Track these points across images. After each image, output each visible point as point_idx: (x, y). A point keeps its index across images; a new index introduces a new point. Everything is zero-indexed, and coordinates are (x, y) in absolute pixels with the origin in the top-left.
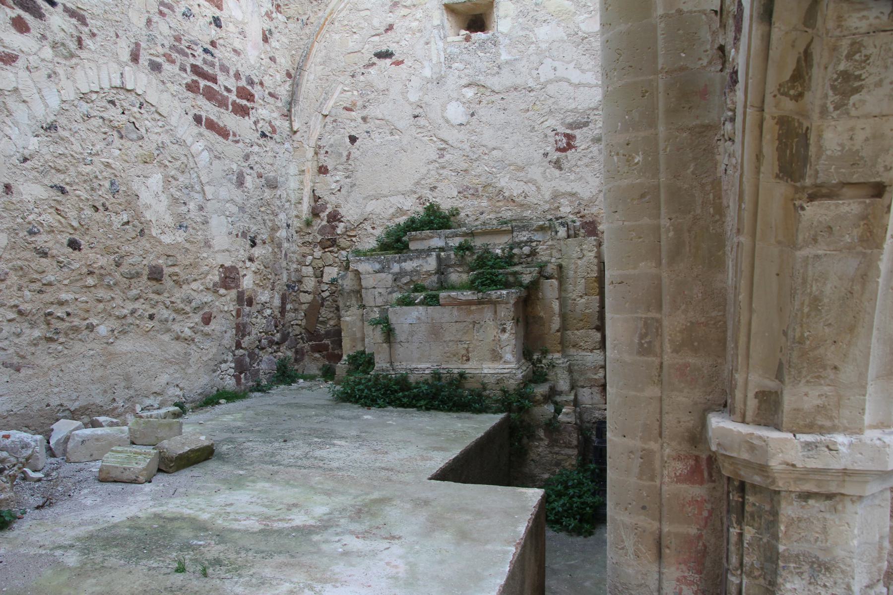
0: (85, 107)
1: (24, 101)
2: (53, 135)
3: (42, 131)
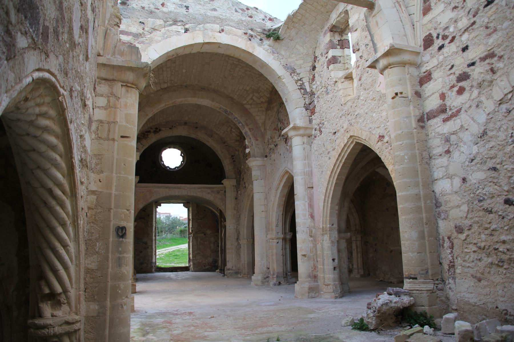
0: (504, 107)
1: (467, 129)
2: (485, 138)
3: (479, 139)
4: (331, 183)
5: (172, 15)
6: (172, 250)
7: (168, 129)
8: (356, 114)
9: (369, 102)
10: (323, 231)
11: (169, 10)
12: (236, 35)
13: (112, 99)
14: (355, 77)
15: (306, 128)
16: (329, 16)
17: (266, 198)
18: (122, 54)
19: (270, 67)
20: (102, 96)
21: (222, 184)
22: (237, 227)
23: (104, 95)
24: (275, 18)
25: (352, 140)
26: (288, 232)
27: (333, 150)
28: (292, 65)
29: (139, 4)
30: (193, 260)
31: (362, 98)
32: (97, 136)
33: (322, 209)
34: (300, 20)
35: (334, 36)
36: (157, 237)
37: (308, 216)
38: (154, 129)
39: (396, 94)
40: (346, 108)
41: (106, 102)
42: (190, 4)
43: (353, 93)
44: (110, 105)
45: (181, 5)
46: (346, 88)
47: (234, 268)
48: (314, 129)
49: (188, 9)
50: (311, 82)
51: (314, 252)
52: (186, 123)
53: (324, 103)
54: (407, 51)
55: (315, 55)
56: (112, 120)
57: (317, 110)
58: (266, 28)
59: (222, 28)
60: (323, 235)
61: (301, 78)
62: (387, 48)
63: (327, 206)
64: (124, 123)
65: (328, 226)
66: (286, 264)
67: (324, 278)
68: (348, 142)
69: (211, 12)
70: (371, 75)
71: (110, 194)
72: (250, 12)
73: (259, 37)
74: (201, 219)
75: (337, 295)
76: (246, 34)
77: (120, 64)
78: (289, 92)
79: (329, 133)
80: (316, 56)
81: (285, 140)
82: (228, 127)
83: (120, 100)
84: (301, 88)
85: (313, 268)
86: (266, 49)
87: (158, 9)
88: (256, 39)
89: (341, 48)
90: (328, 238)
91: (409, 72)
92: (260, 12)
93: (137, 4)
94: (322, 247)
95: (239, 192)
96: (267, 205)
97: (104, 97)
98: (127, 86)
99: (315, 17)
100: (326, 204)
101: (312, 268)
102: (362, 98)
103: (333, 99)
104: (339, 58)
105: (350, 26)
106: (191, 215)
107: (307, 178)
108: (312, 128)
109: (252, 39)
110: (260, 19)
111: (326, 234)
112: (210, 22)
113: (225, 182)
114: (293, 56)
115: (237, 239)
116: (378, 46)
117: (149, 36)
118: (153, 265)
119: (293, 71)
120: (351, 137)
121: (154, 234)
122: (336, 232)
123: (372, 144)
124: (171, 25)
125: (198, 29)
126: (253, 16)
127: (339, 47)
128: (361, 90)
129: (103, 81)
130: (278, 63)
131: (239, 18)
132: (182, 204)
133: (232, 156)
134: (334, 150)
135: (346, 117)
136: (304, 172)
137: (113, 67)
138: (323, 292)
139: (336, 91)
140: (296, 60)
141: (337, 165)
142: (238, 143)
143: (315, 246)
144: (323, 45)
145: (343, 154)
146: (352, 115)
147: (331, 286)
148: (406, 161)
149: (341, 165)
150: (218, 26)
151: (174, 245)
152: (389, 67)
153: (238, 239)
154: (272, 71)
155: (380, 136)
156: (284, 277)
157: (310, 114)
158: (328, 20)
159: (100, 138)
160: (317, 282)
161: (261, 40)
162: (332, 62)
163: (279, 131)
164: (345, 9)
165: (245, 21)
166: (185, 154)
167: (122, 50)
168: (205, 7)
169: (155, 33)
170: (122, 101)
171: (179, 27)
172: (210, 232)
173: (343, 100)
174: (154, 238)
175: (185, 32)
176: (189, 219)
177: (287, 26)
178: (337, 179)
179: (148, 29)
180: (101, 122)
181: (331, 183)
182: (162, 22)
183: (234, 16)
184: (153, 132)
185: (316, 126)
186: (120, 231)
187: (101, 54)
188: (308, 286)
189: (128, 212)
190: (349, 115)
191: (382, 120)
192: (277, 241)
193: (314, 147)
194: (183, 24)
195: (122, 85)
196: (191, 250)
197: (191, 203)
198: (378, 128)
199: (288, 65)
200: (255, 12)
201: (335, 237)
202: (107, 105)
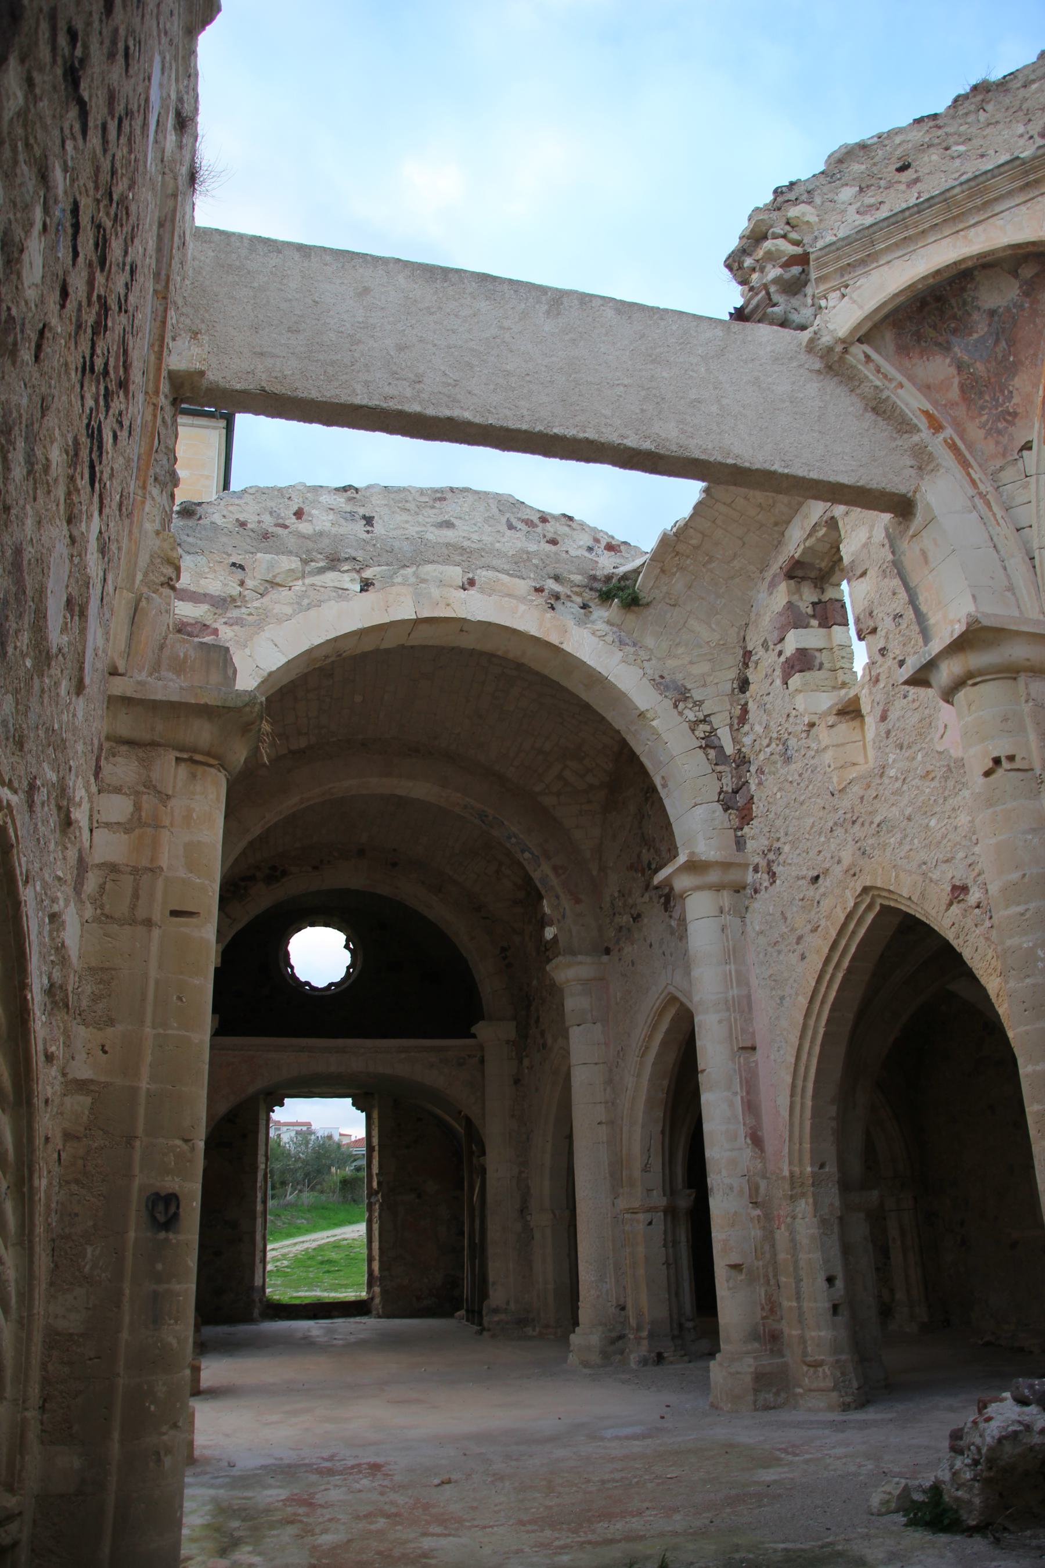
4: (810, 1033)
5: (326, 541)
6: (314, 1245)
8: (877, 820)
9: (914, 783)
10: (792, 1188)
11: (317, 528)
12: (509, 595)
13: (148, 801)
14: (869, 709)
15: (726, 866)
16: (783, 534)
17: (610, 1082)
18: (179, 667)
19: (613, 687)
20: (118, 790)
21: (474, 1036)
22: (521, 1172)
23: (125, 790)
24: (625, 543)
25: (868, 900)
26: (680, 1187)
27: (812, 931)
28: (679, 676)
29: (231, 512)
30: (382, 1279)
31: (892, 773)
32: (99, 911)
33: (787, 1117)
34: (696, 548)
35: (798, 591)
36: (270, 1203)
37: (742, 1140)
39: (997, 761)
40: (845, 803)
41: (131, 809)
42: (377, 509)
43: (866, 757)
44: (140, 819)
45: (352, 514)
46: (843, 744)
47: (512, 1306)
48: (751, 869)
49: (372, 526)
50: (736, 727)
51: (768, 1256)
52: (361, 853)
53: (780, 789)
54: (1018, 634)
55: (745, 647)
56: (145, 863)
57: (757, 809)
58: (599, 573)
59: (470, 576)
60: (793, 1198)
61: (706, 716)
62: (959, 629)
63: (803, 1105)
64: (182, 873)
65: (809, 1169)
66: (677, 1294)
67: (802, 1340)
68: (856, 905)
69: (436, 531)
70: (916, 704)
71: (134, 1091)
72: (552, 530)
73: (579, 600)
75: (848, 1399)
76: (539, 590)
77: (175, 698)
78: (673, 758)
79: (798, 878)
80: (749, 648)
81: (662, 900)
83: (173, 803)
84: (707, 746)
85: (767, 1308)
86: (599, 633)
87: (286, 527)
88: (569, 604)
89: (820, 625)
90: (810, 1209)
91: (1028, 694)
92: (578, 527)
93: (225, 513)
94: (793, 1240)
95: (526, 1062)
96: (613, 1103)
97: (125, 794)
98: (191, 760)
99: (741, 539)
100: (798, 1099)
101: (763, 1309)
102: (892, 773)
103: (806, 775)
104: (817, 654)
105: (846, 560)
106: (375, 1133)
107: (736, 1020)
108: (747, 865)
109: (558, 606)
110: (580, 547)
111: (803, 1195)
112: (436, 558)
113: (483, 1030)
114: (680, 651)
115: (522, 1211)
116: (932, 621)
117: (256, 604)
119: (682, 696)
120: (866, 890)
121: (259, 1195)
122: (835, 1190)
123: (933, 913)
124: (321, 571)
125: (399, 580)
126: (559, 539)
127: (814, 622)
128: (888, 750)
129: (124, 748)
130: (635, 672)
131: (519, 545)
132: (349, 1100)
133: (503, 950)
134: (815, 930)
135: (846, 831)
136: (726, 1001)
137: (154, 707)
138: (800, 1390)
139: (812, 753)
140: (691, 663)
141: (828, 977)
143: (769, 1237)
144: (768, 619)
145: (843, 942)
146: (867, 824)
147: (826, 1368)
148: (1040, 965)
149: (840, 976)
150: (459, 569)
151: (324, 1229)
152: (970, 682)
153: (523, 1211)
154: (617, 697)
155: (954, 888)
156: (673, 1338)
157: (736, 822)
158: (779, 544)
159: (107, 917)
160: (783, 1356)
161: (584, 606)
162: (797, 668)
163: (643, 875)
164: (829, 514)
165: (536, 553)
166: (356, 944)
167: (182, 655)
168: (420, 518)
169: (274, 594)
170: (177, 804)
171: (346, 575)
173: (835, 780)
174: (259, 1207)
175: (362, 590)
177: (660, 565)
178: (828, 1021)
179: (256, 583)
180: (112, 868)
181: (810, 1033)
182: (295, 563)
183: (504, 540)
185: (757, 859)
186: (161, 1207)
187: (121, 670)
188: (752, 1370)
189: (185, 1147)
190: (857, 826)
191: (958, 839)
192: (648, 1216)
193: (755, 922)
194: (358, 567)
195: (177, 759)
196: (376, 1245)
198: (947, 861)
199: (668, 678)
200: (567, 529)
201: (832, 1204)
202: (130, 820)
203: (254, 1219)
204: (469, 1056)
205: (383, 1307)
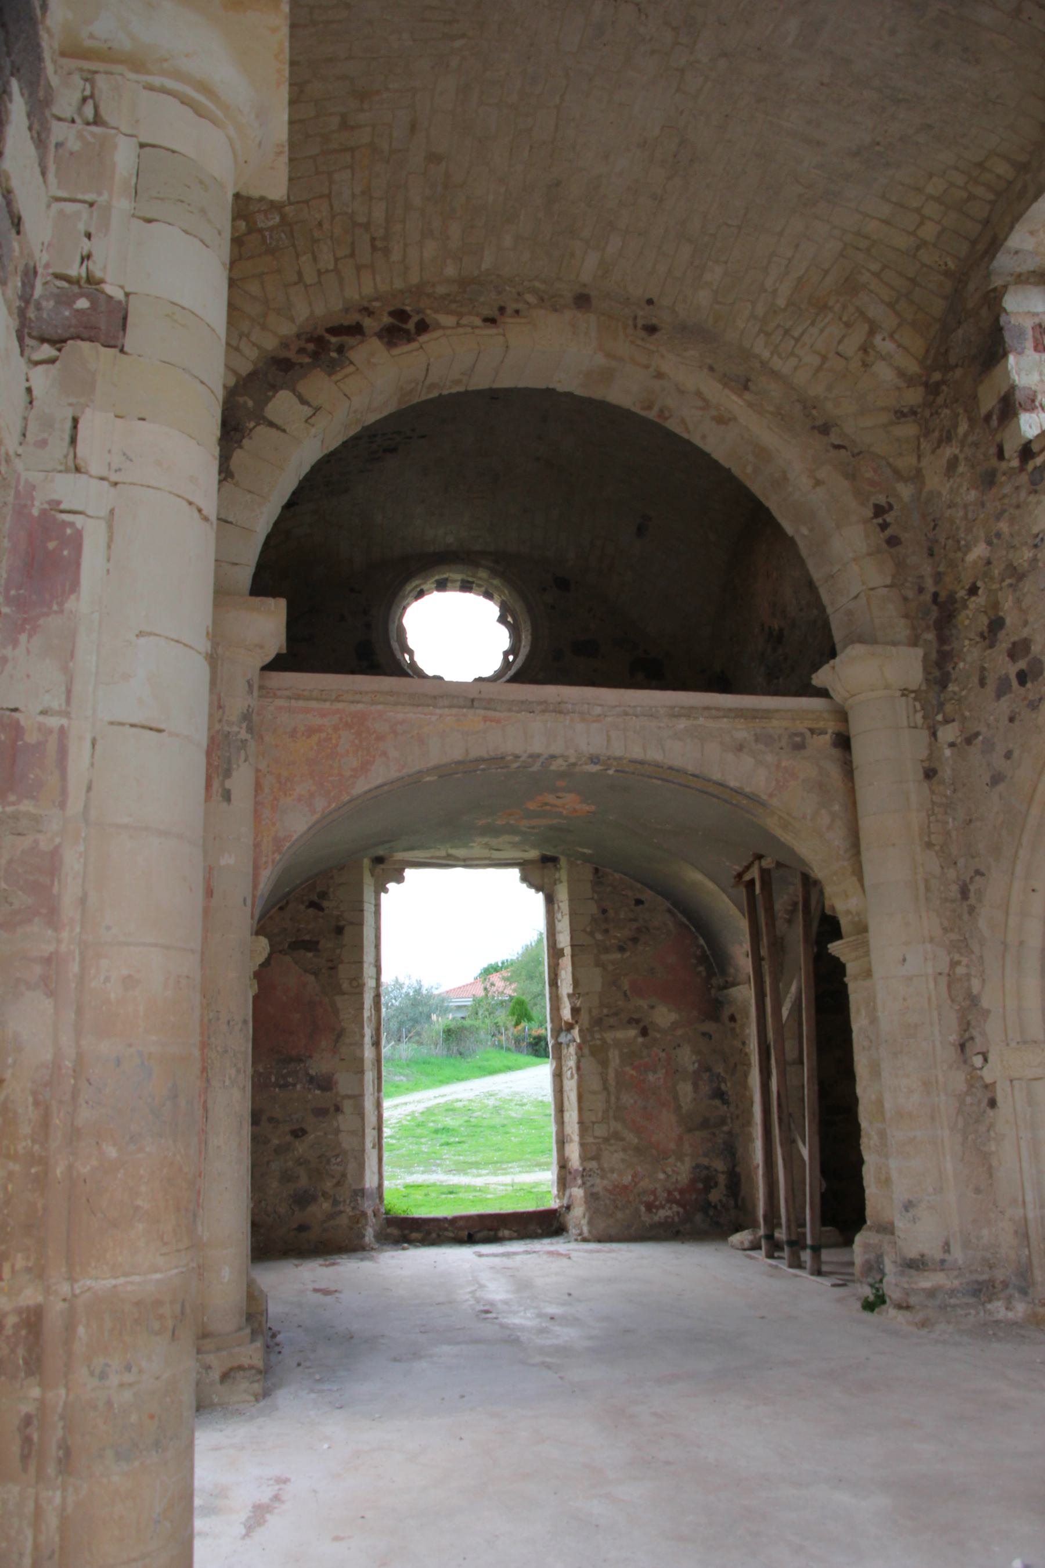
6: (421, 1107)
7: (478, 322)
22: (954, 964)
30: (585, 1174)
36: (386, 1050)
38: (387, 320)
52: (582, 301)
74: (622, 949)
82: (848, 325)
106: (564, 926)
118: (368, 1206)
121: (368, 1032)
132: (515, 873)
133: (879, 510)
142: (909, 430)
151: (427, 1087)
172: (673, 1017)
174: (369, 1053)
176: (555, 953)
184: (380, 335)
196: (572, 1116)
197: (563, 862)
203: (362, 1072)
204: (812, 731)
205: (590, 1223)
